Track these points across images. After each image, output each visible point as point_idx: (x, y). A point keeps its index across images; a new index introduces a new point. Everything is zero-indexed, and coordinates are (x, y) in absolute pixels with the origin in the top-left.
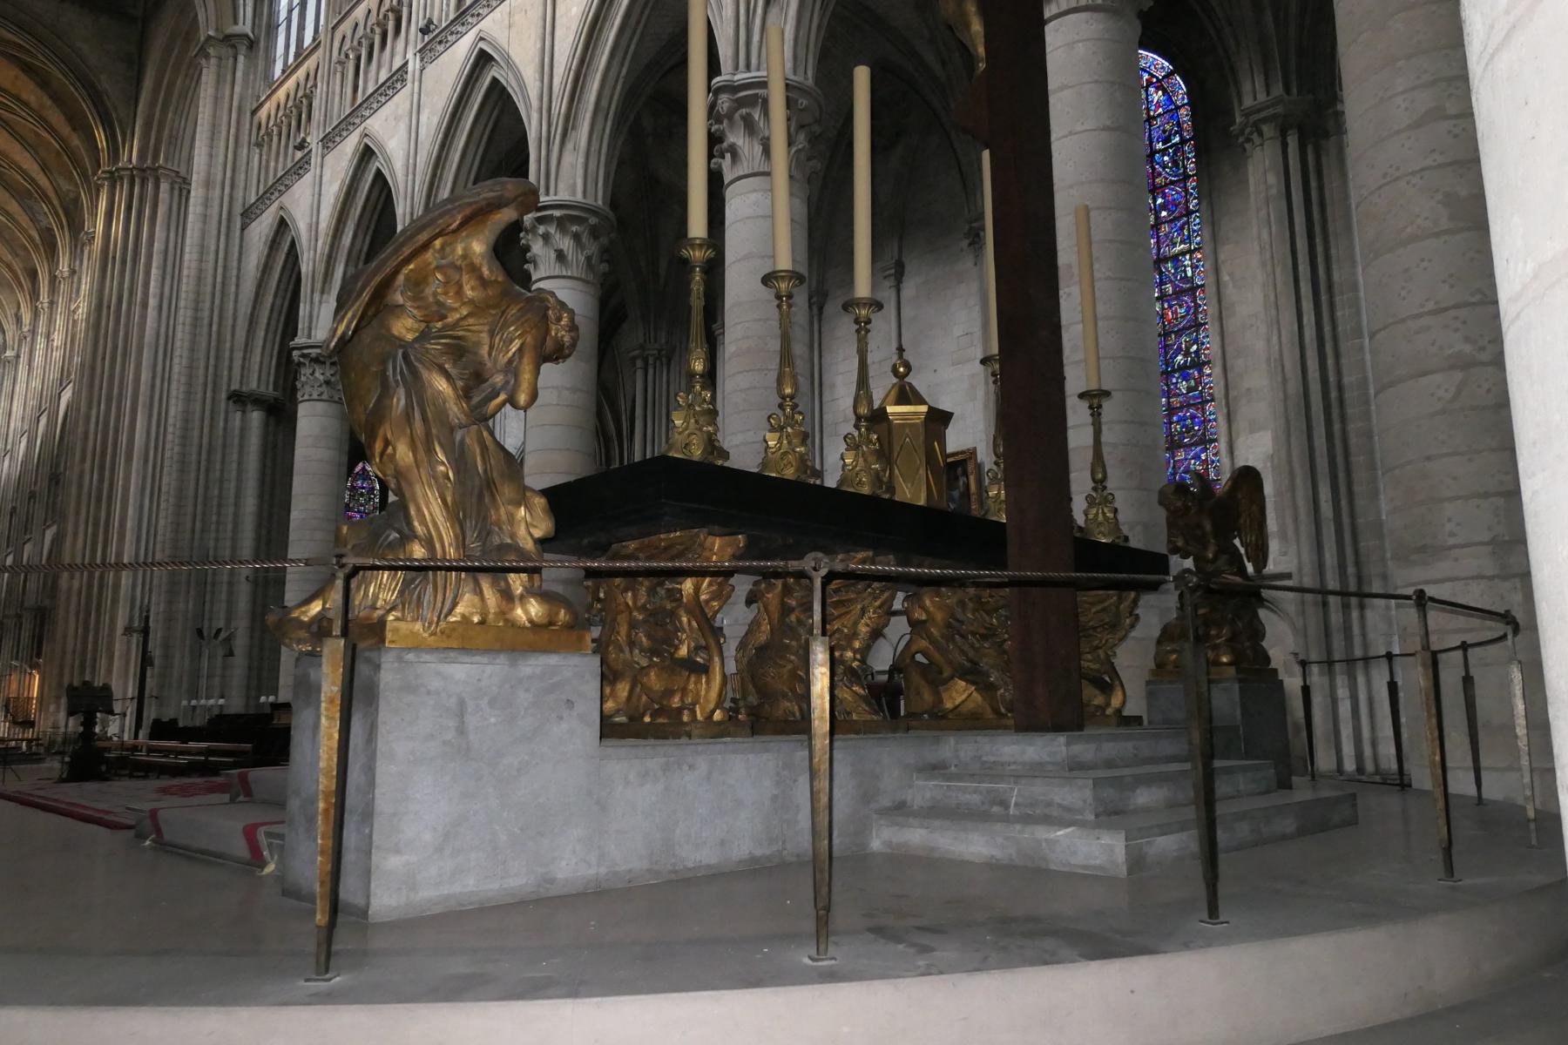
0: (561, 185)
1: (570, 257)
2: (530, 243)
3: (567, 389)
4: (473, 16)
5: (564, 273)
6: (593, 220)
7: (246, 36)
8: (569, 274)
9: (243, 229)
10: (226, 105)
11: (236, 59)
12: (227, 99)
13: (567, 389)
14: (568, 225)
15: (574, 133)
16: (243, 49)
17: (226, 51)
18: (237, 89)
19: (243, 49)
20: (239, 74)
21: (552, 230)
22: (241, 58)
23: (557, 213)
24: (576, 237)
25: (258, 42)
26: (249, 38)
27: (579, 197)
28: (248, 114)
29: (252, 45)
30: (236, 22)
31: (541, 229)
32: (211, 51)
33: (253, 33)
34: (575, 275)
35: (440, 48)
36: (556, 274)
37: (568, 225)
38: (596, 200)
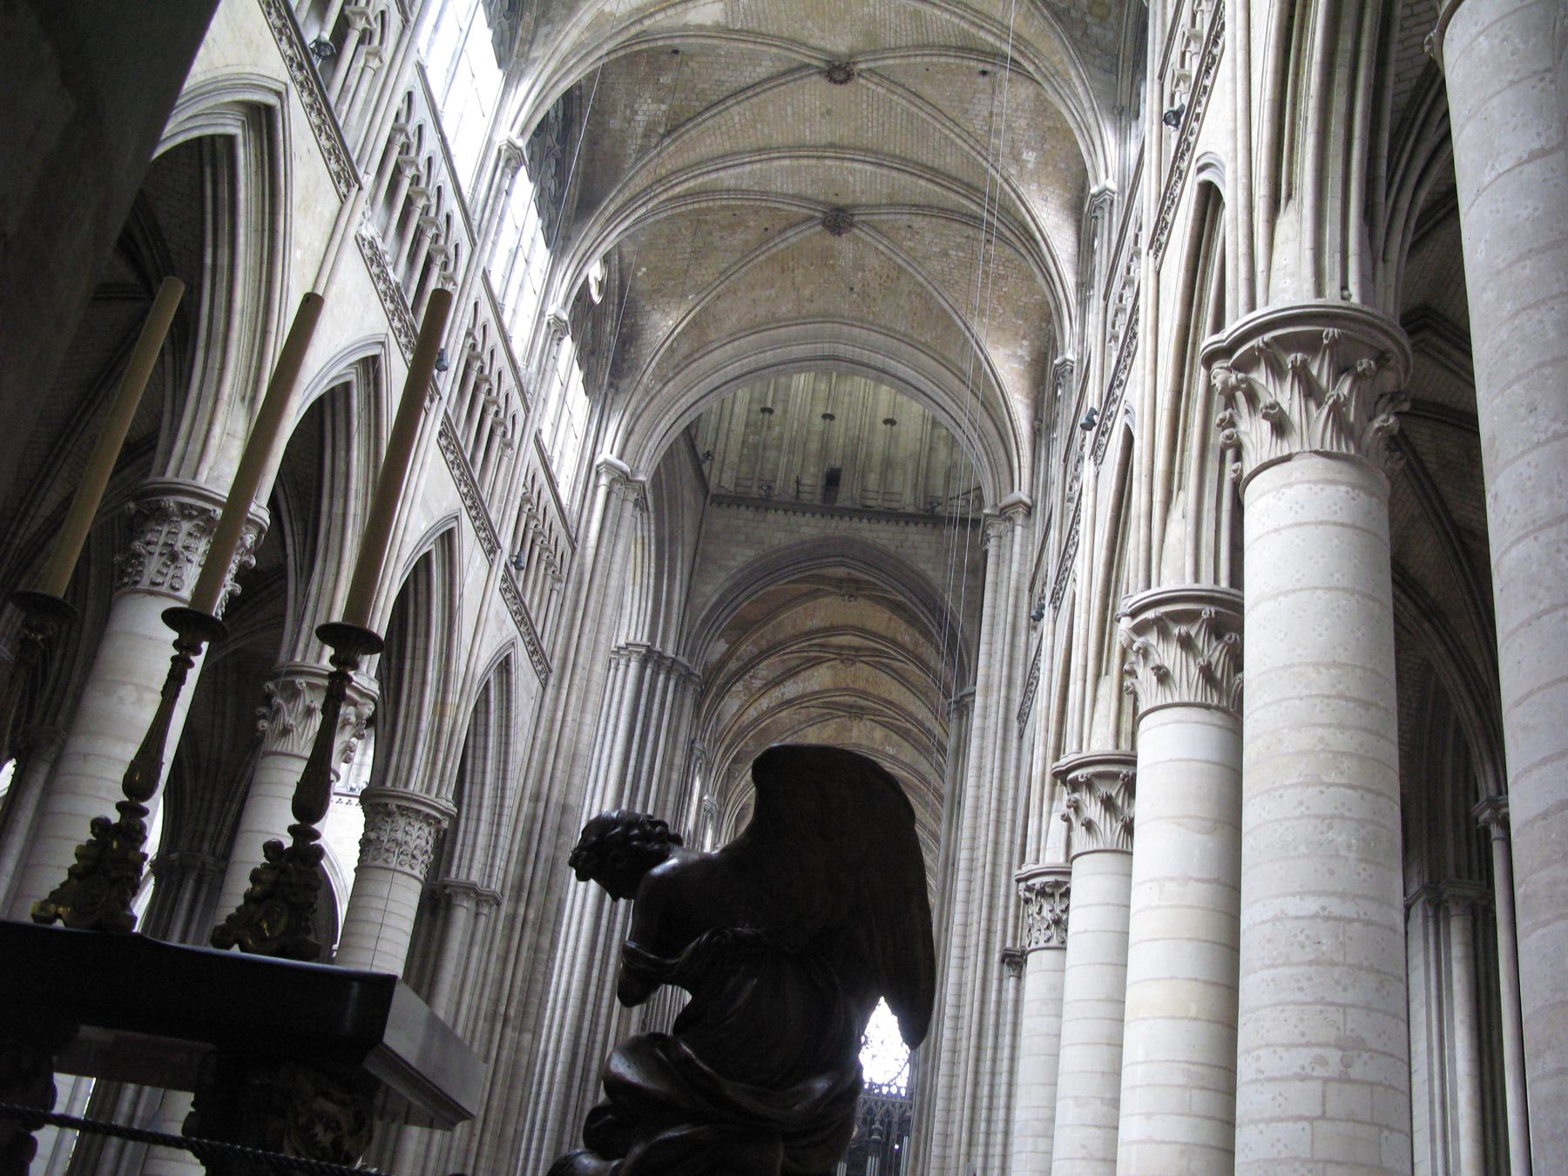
0: (1165, 572)
1: (1177, 676)
2: (1135, 667)
3: (1172, 879)
4: (1118, 386)
5: (1169, 701)
6: (1208, 611)
7: (1021, 502)
8: (1177, 700)
9: (1021, 737)
10: (1004, 590)
11: (1013, 531)
12: (1005, 581)
13: (1172, 879)
14: (1171, 625)
15: (1182, 494)
16: (1020, 519)
17: (1003, 527)
18: (1015, 567)
19: (1020, 519)
20: (1017, 548)
21: (1152, 638)
22: (1018, 530)
23: (1150, 614)
24: (1186, 643)
25: (1034, 505)
26: (1025, 504)
27: (1188, 583)
28: (1027, 592)
29: (1029, 511)
30: (1013, 490)
31: (1139, 641)
32: (991, 532)
33: (1031, 497)
34: (1186, 699)
35: (1104, 440)
36: (1159, 704)
37: (1171, 625)
38: (1216, 581)
